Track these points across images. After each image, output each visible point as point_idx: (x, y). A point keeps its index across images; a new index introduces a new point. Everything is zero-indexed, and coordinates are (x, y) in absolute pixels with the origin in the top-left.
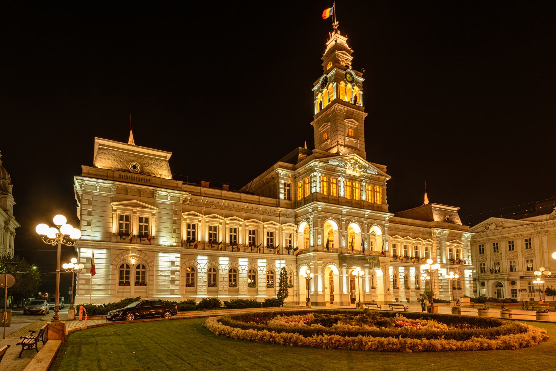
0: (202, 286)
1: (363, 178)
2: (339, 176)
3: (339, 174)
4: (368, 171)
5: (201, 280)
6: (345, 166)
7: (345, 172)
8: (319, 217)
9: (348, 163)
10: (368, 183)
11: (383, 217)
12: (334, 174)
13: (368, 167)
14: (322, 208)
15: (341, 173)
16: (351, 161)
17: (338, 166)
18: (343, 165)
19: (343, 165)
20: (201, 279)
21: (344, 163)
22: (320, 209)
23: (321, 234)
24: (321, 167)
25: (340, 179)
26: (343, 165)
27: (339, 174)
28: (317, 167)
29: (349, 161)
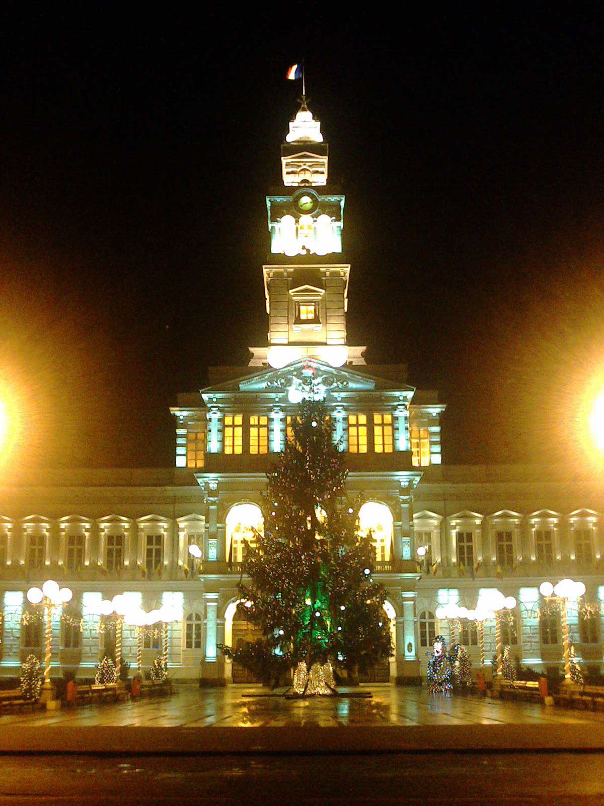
0: (11, 645)
1: (338, 402)
2: (271, 410)
3: (271, 405)
4: (352, 385)
5: (10, 635)
6: (285, 387)
7: (285, 400)
8: (213, 503)
9: (294, 378)
10: (352, 410)
11: (394, 481)
12: (256, 407)
13: (348, 376)
14: (217, 484)
15: (278, 402)
16: (302, 374)
17: (268, 390)
18: (282, 384)
19: (282, 384)
20: (9, 632)
21: (283, 381)
22: (213, 486)
23: (219, 535)
24: (219, 400)
25: (273, 415)
26: (280, 386)
27: (271, 405)
28: (213, 402)
29: (295, 373)
